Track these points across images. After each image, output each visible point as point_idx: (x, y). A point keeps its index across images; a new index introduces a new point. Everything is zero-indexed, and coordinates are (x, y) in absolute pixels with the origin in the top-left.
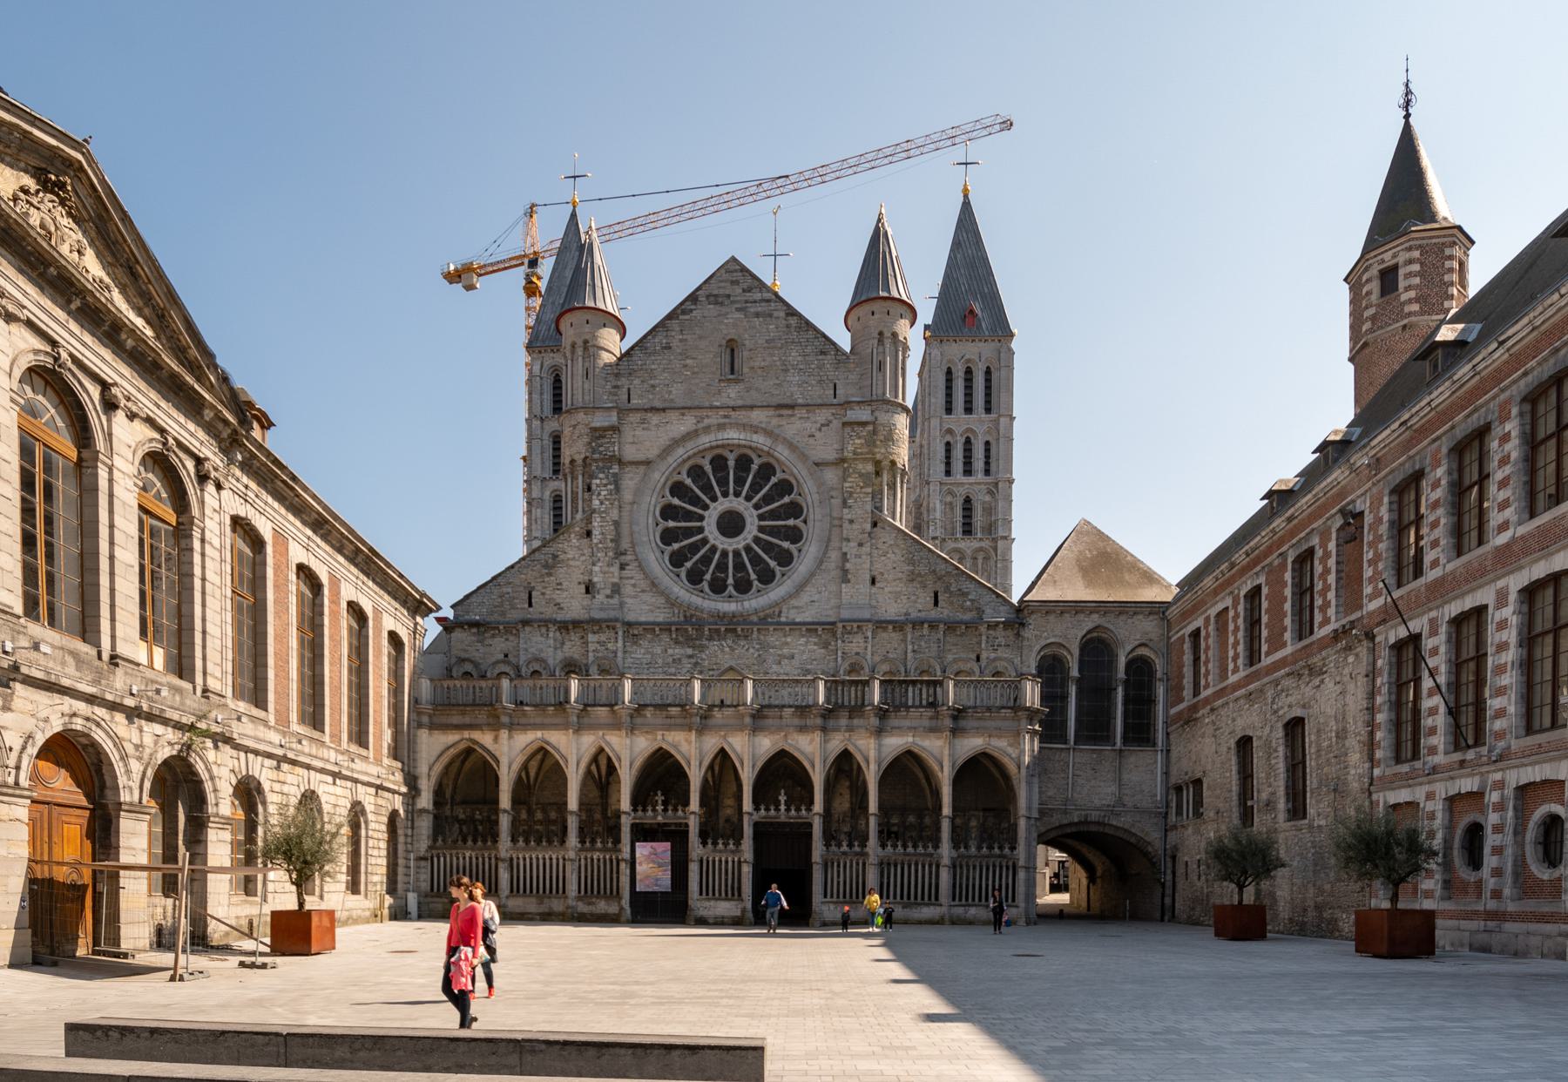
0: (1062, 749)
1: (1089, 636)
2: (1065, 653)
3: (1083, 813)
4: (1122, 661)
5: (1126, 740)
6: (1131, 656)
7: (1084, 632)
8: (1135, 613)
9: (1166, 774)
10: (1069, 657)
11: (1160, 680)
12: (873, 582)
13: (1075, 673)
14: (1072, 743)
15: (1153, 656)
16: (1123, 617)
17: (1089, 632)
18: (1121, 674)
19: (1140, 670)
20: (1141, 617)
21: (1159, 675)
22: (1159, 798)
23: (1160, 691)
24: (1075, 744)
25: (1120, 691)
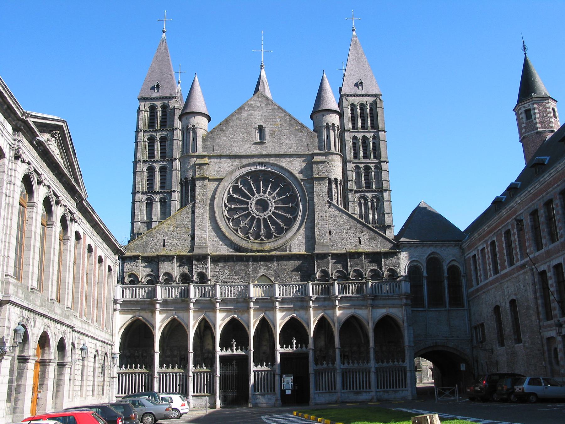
0: (422, 310)
1: (430, 257)
2: (420, 265)
3: (434, 341)
6: (449, 265)
8: (449, 246)
9: (470, 320)
10: (422, 267)
11: (463, 276)
12: (330, 233)
13: (425, 274)
15: (458, 265)
16: (444, 248)
17: (430, 255)
19: (453, 270)
21: (462, 274)
22: (468, 332)
23: (463, 281)
24: (428, 308)
25: (446, 282)
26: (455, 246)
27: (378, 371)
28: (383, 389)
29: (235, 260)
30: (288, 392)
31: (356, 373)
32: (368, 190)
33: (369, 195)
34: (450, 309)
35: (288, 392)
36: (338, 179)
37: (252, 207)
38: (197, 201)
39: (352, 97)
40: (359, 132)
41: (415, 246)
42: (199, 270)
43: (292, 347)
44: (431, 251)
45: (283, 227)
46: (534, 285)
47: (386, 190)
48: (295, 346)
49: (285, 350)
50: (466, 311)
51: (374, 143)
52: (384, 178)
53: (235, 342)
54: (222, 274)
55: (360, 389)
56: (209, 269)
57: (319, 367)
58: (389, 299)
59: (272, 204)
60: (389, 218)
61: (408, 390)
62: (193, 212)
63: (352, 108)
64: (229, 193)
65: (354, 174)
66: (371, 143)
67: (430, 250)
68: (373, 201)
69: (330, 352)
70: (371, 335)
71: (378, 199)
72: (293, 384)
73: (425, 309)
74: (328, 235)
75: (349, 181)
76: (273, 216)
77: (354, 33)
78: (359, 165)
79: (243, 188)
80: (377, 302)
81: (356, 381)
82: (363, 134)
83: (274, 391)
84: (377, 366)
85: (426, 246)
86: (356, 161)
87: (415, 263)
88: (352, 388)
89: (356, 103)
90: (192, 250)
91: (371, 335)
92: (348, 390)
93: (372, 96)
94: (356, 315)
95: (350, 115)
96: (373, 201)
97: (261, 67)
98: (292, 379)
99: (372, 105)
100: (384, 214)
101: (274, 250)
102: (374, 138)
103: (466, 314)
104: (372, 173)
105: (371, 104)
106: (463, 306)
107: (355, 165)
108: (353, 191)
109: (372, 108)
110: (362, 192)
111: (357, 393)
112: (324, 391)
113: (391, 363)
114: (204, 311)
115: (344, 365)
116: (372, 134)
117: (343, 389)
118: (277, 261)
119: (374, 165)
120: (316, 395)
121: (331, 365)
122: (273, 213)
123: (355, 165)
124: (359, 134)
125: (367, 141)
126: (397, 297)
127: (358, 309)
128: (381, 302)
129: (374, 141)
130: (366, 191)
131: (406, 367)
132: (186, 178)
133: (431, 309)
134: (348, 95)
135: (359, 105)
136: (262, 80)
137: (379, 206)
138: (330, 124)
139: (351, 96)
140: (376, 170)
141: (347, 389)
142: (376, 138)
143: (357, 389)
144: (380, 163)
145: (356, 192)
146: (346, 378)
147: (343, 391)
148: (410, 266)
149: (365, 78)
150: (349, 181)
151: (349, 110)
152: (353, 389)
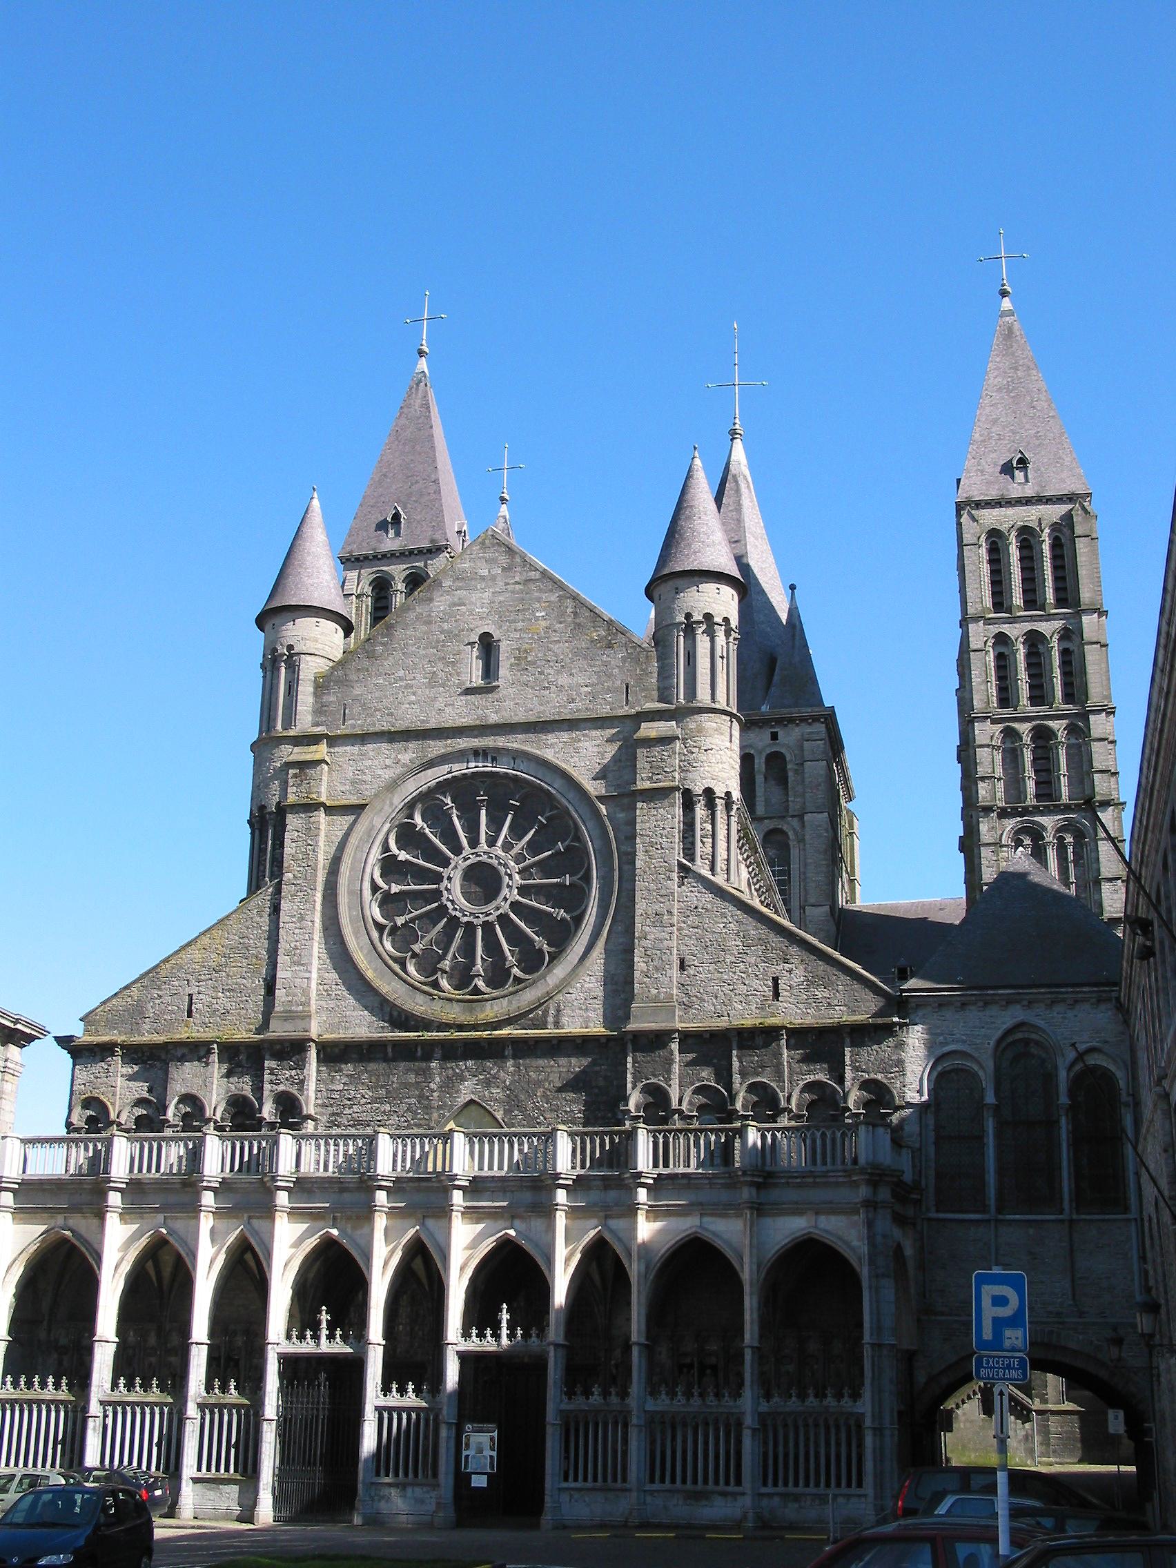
0: (977, 1221)
1: (1010, 1039)
2: (976, 1068)
4: (1063, 1074)
5: (1079, 1201)
7: (999, 1033)
8: (1076, 1001)
10: (981, 1073)
11: (1127, 1105)
12: (682, 966)
13: (990, 1098)
14: (993, 1209)
15: (1112, 1068)
16: (1059, 1008)
18: (1064, 1099)
20: (1087, 1006)
21: (1124, 1097)
24: (999, 1210)
26: (1099, 1001)
27: (765, 1423)
28: (780, 1489)
29: (390, 1054)
30: (480, 1481)
31: (707, 1424)
32: (1044, 806)
33: (1049, 822)
34: (1075, 1217)
35: (480, 1481)
36: (716, 789)
37: (454, 890)
38: (288, 876)
39: (993, 507)
40: (1014, 620)
41: (959, 1004)
42: (281, 1088)
43: (497, 1336)
44: (1015, 1021)
45: (541, 951)
46: (1170, 1150)
47: (1106, 804)
48: (504, 1332)
49: (473, 1344)
50: (1133, 1223)
51: (1065, 653)
52: (1097, 765)
53: (327, 1313)
54: (349, 1099)
55: (706, 1481)
56: (312, 1085)
57: (579, 1403)
58: (815, 1185)
59: (510, 876)
60: (1115, 896)
61: (865, 1496)
62: (276, 909)
63: (994, 543)
64: (386, 848)
65: (998, 757)
66: (1056, 655)
67: (1006, 1019)
68: (1061, 840)
69: (660, 1353)
70: (750, 1303)
71: (1079, 835)
72: (494, 1454)
73: (986, 1217)
74: (675, 972)
75: (983, 779)
76: (512, 916)
77: (1006, 304)
78: (1016, 725)
79: (427, 831)
80: (775, 1194)
81: (684, 1452)
82: (1028, 626)
83: (435, 1475)
84: (764, 1407)
85: (994, 1002)
86: (1007, 712)
87: (946, 1064)
88: (679, 1479)
89: (1003, 528)
90: (264, 1026)
91: (750, 1303)
92: (667, 1485)
93: (1059, 500)
94: (707, 1236)
95: (986, 568)
96: (1061, 840)
97: (733, 434)
98: (492, 1439)
99: (1060, 531)
100: (1097, 882)
101: (509, 1021)
102: (1066, 635)
103: (1134, 1235)
104: (1057, 748)
105: (1055, 527)
106: (1126, 1209)
107: (1000, 726)
108: (993, 811)
109: (1060, 540)
110: (1025, 812)
111: (698, 1496)
112: (590, 1484)
113: (811, 1401)
114: (246, 1216)
115: (659, 1401)
116: (1058, 624)
117: (652, 1481)
118: (515, 1057)
119: (1065, 722)
120: (565, 1497)
121: (614, 1399)
122: (515, 906)
123: (1000, 726)
124: (1017, 625)
125: (1041, 648)
126: (841, 1179)
127: (712, 1215)
128: (791, 1195)
129: (1067, 645)
130: (1037, 811)
131: (863, 1414)
132: (262, 808)
133: (1011, 1217)
134: (978, 505)
135: (1014, 533)
136: (734, 476)
137: (1082, 858)
138: (697, 617)
139: (989, 504)
140: (1073, 741)
141: (662, 1481)
142: (1074, 636)
143: (695, 1482)
144: (1084, 716)
145: (1003, 814)
146: (706, 1443)
147: (648, 1487)
148: (939, 1068)
149: (1037, 442)
150: (983, 779)
151: (983, 551)
152: (684, 1481)
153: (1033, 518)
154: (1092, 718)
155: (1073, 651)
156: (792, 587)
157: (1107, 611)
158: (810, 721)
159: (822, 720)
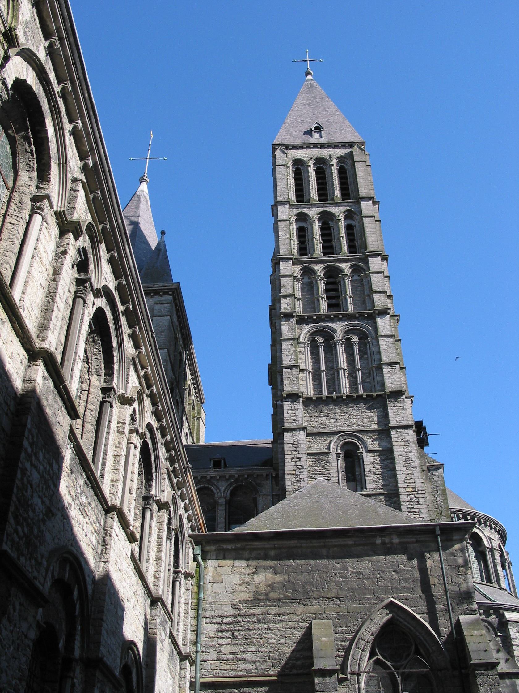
33: (339, 327)
39: (297, 149)
47: (384, 312)
51: (349, 228)
52: (375, 288)
60: (395, 377)
65: (298, 286)
66: (343, 230)
68: (348, 340)
71: (363, 337)
75: (285, 296)
77: (309, 77)
82: (321, 209)
86: (304, 259)
93: (343, 145)
95: (292, 181)
96: (348, 340)
97: (142, 180)
100: (379, 368)
102: (349, 215)
104: (344, 280)
105: (341, 159)
107: (299, 267)
108: (293, 317)
110: (319, 319)
116: (343, 209)
119: (349, 264)
123: (299, 267)
124: (314, 209)
125: (331, 224)
129: (350, 222)
130: (328, 318)
134: (287, 147)
136: (139, 197)
137: (366, 354)
140: (356, 277)
145: (301, 321)
150: (285, 296)
151: (291, 171)
153: (326, 155)
154: (370, 260)
155: (355, 226)
156: (163, 233)
157: (379, 202)
158: (161, 293)
159: (170, 293)
